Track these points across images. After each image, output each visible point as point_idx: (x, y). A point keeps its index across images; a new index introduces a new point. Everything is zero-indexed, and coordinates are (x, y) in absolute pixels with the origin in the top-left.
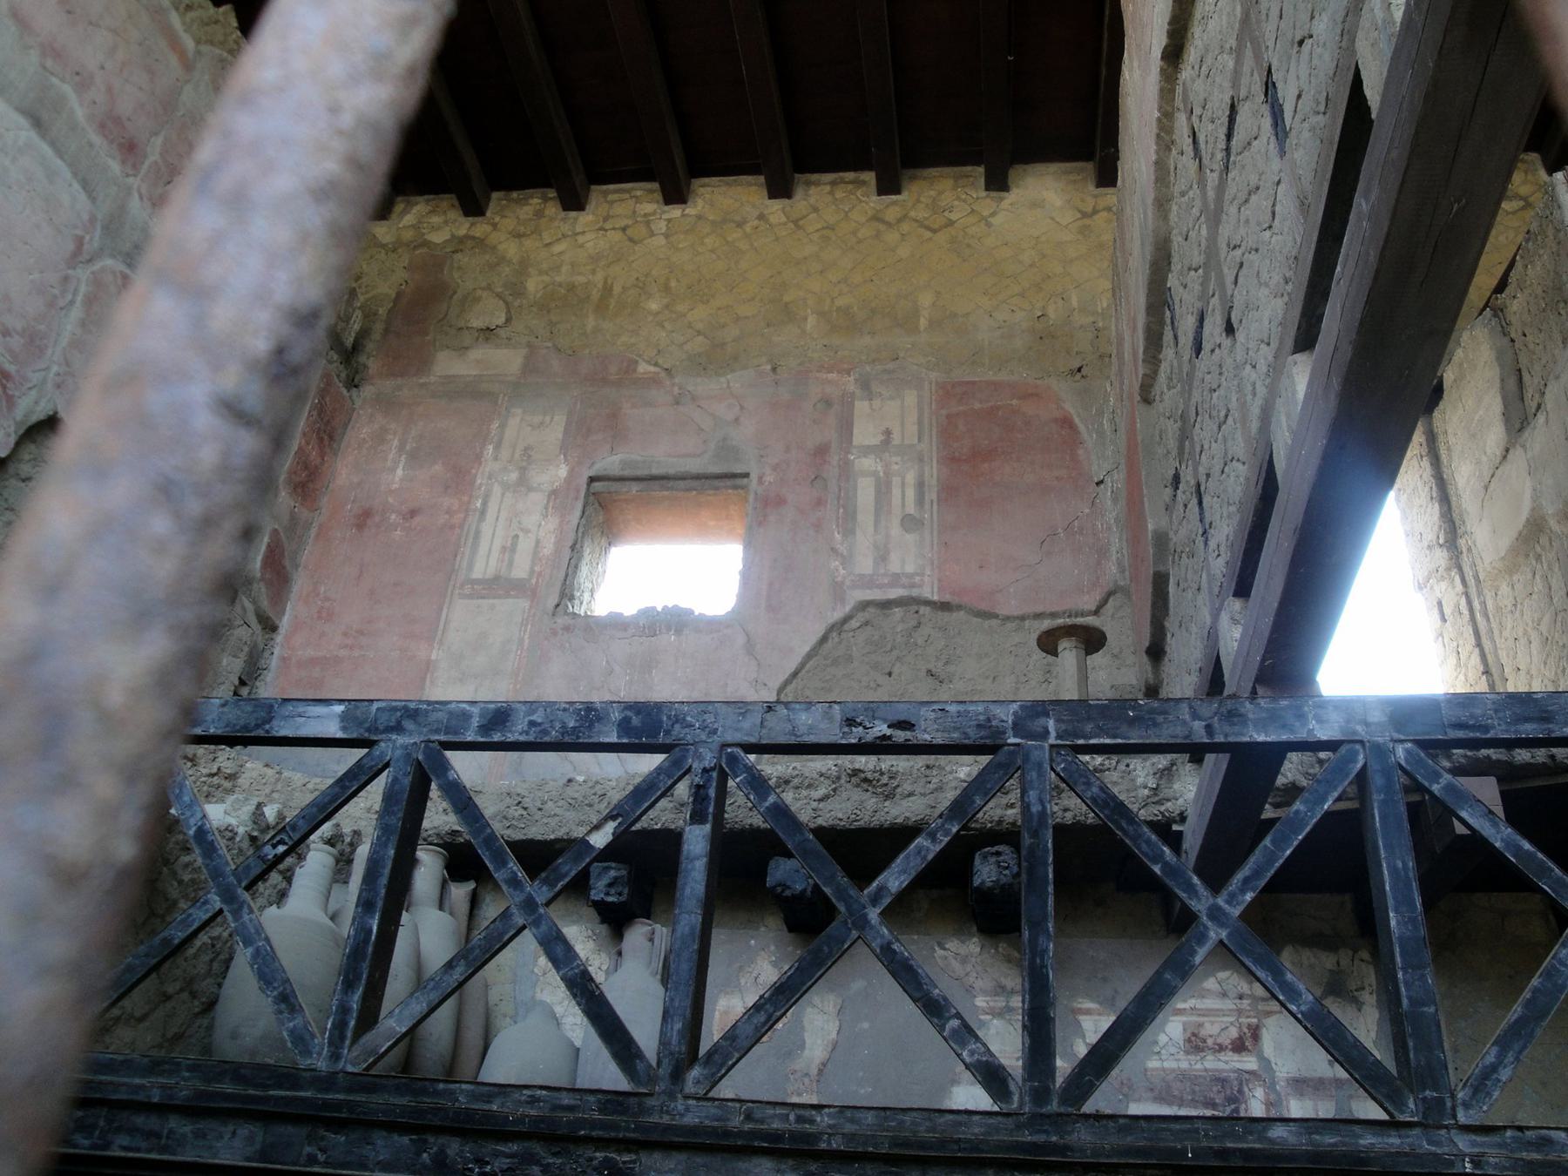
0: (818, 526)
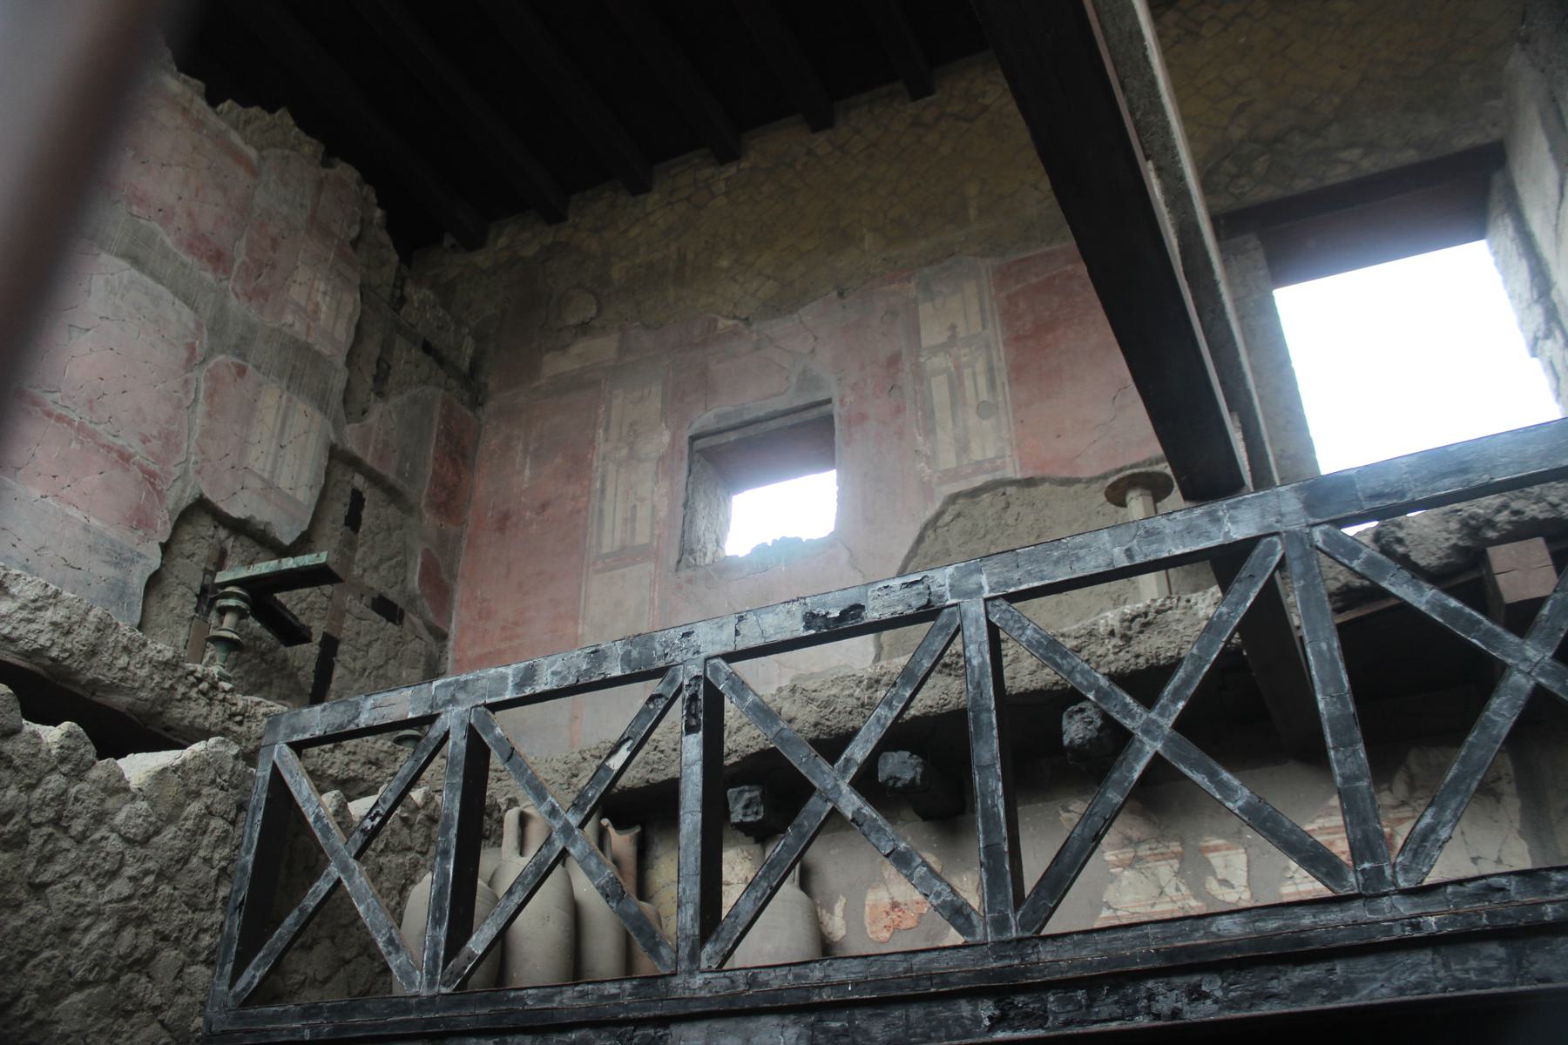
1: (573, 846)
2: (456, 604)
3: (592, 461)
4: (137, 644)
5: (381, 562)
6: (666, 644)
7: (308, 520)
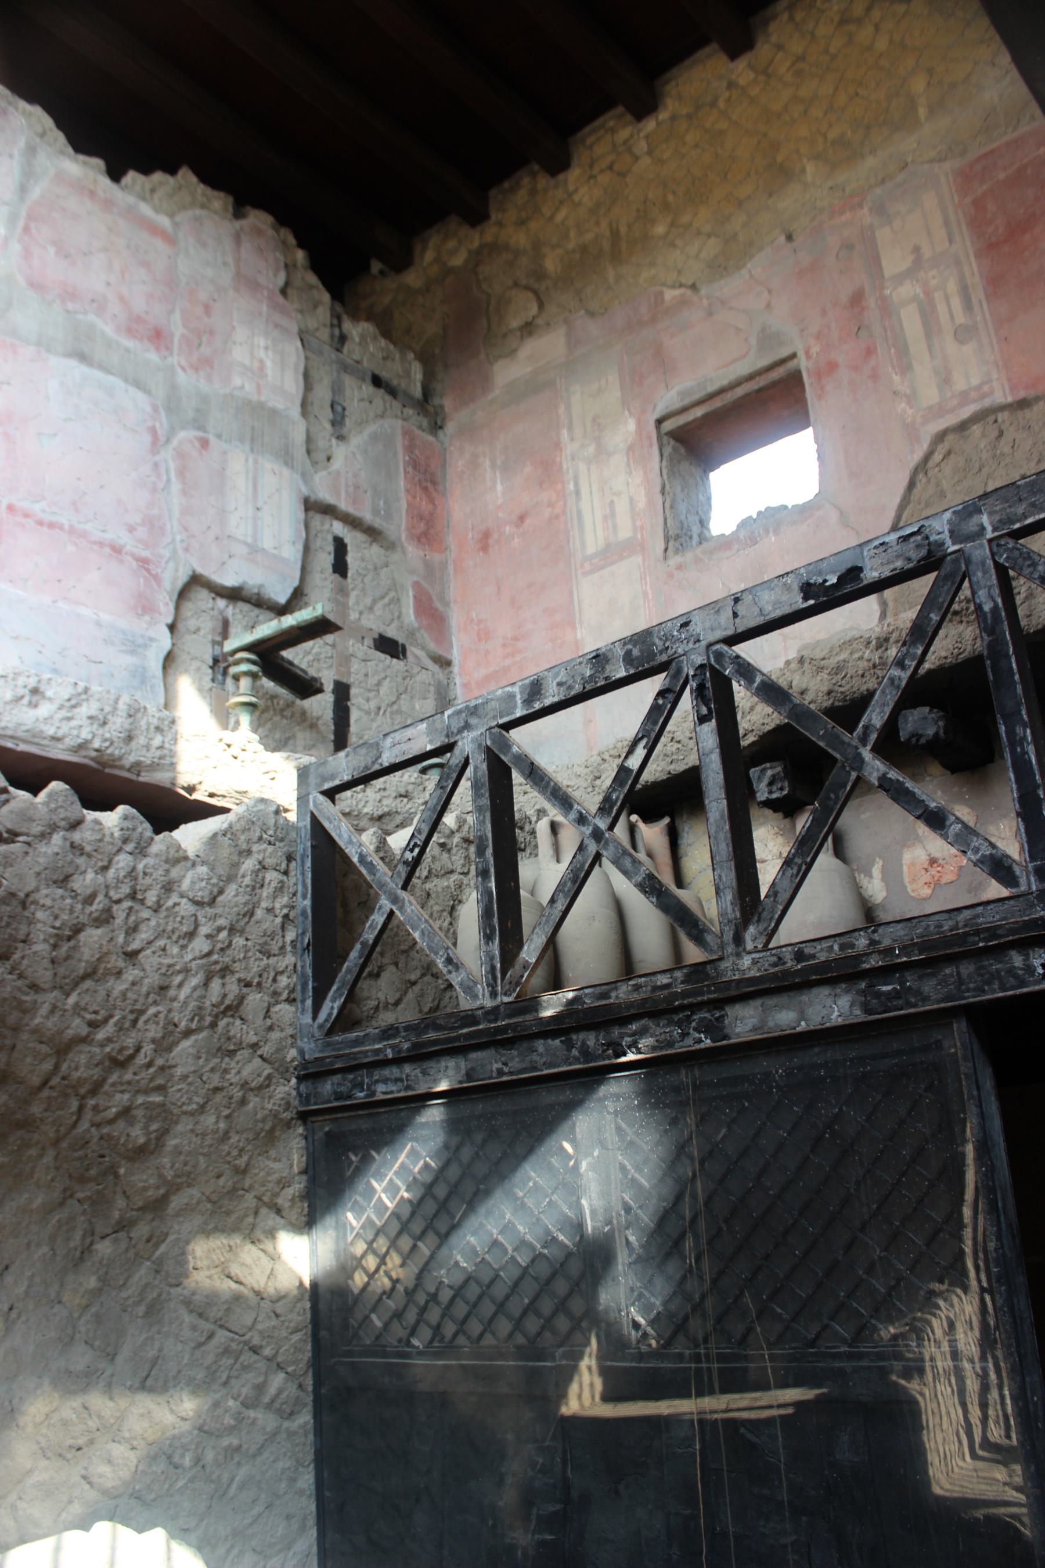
0: (875, 376)
1: (606, 849)
2: (454, 630)
3: (561, 463)
4: (166, 723)
5: (375, 602)
6: (666, 638)
7: (297, 574)
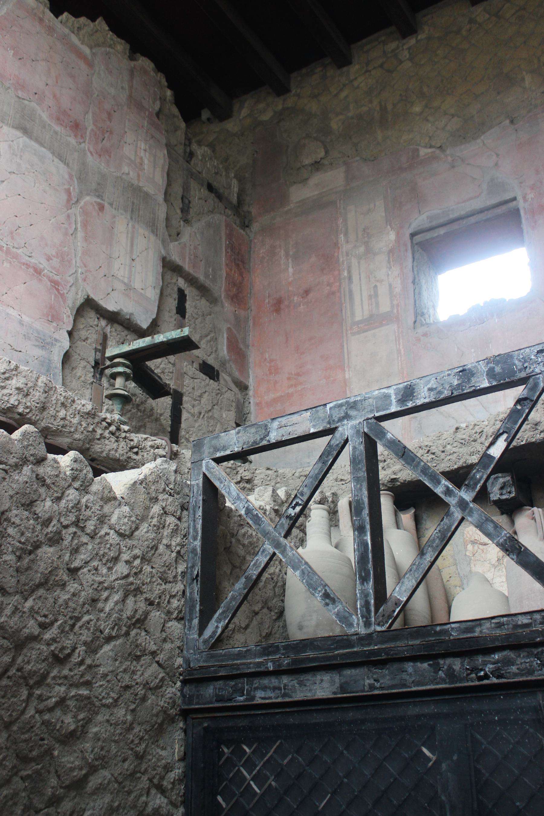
1: (471, 516)
2: (251, 365)
3: (338, 257)
